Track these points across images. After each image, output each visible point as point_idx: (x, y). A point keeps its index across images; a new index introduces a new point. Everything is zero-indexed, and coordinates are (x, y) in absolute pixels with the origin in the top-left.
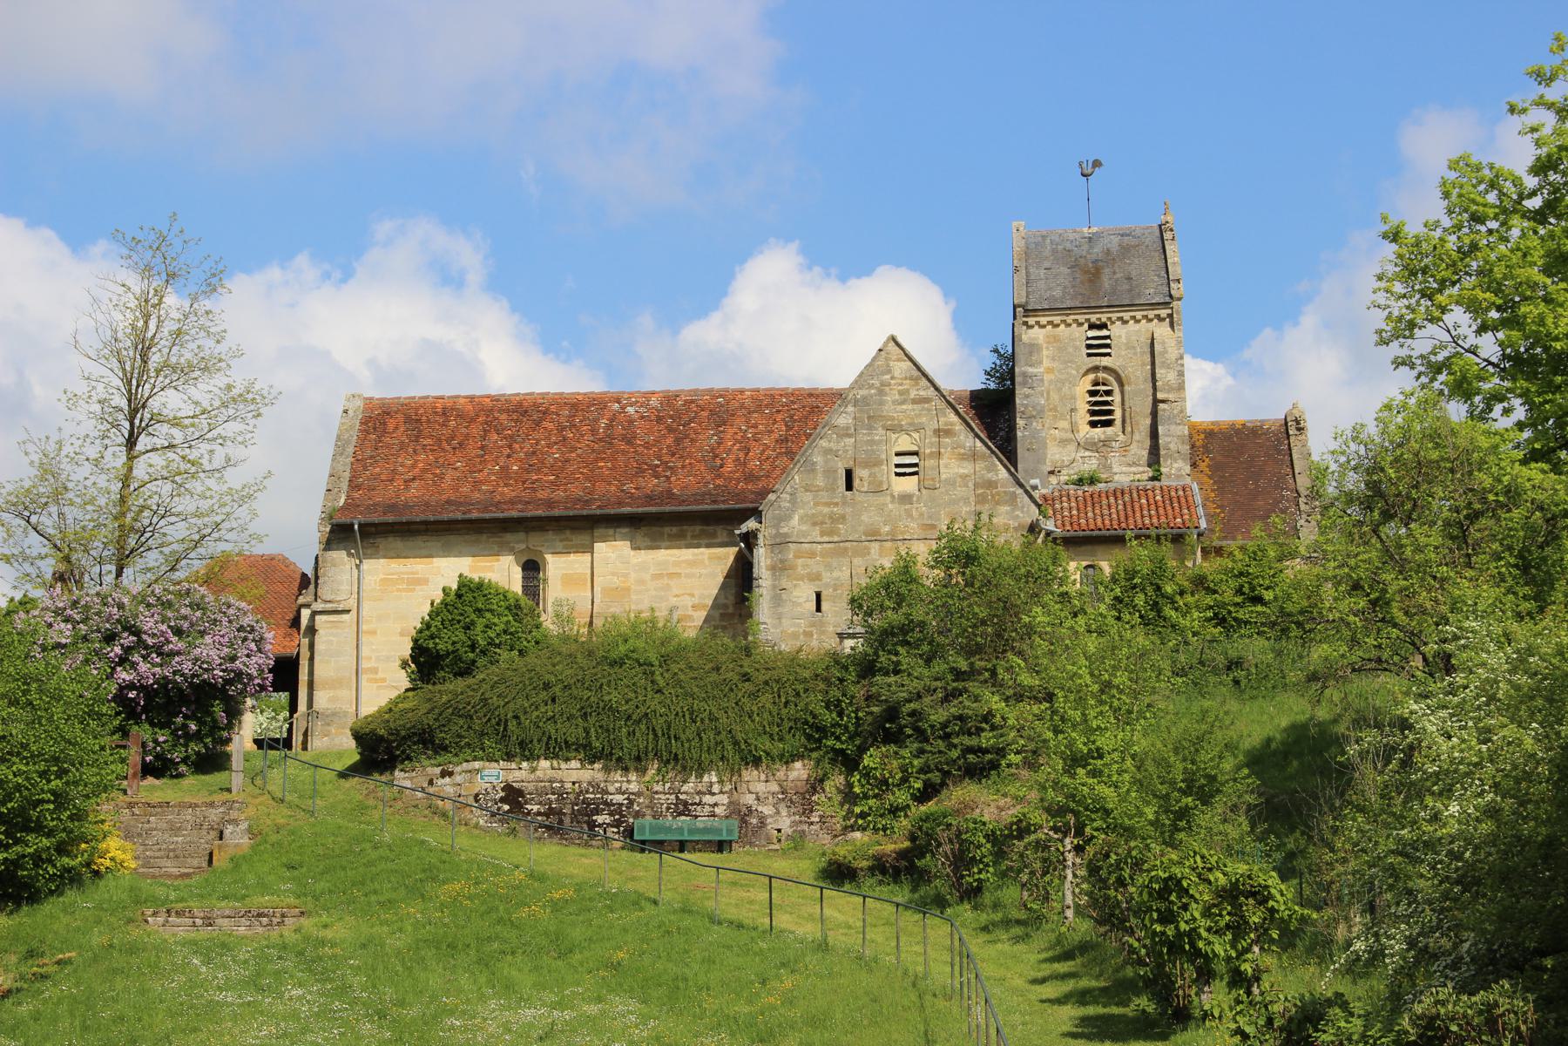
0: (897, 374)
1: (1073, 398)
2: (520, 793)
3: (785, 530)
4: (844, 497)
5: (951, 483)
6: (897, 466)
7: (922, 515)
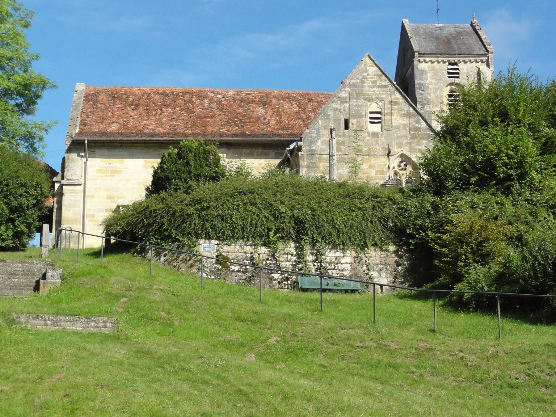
0: (370, 73)
1: (442, 97)
2: (227, 258)
3: (314, 148)
4: (344, 132)
5: (397, 128)
6: (371, 118)
7: (383, 143)
